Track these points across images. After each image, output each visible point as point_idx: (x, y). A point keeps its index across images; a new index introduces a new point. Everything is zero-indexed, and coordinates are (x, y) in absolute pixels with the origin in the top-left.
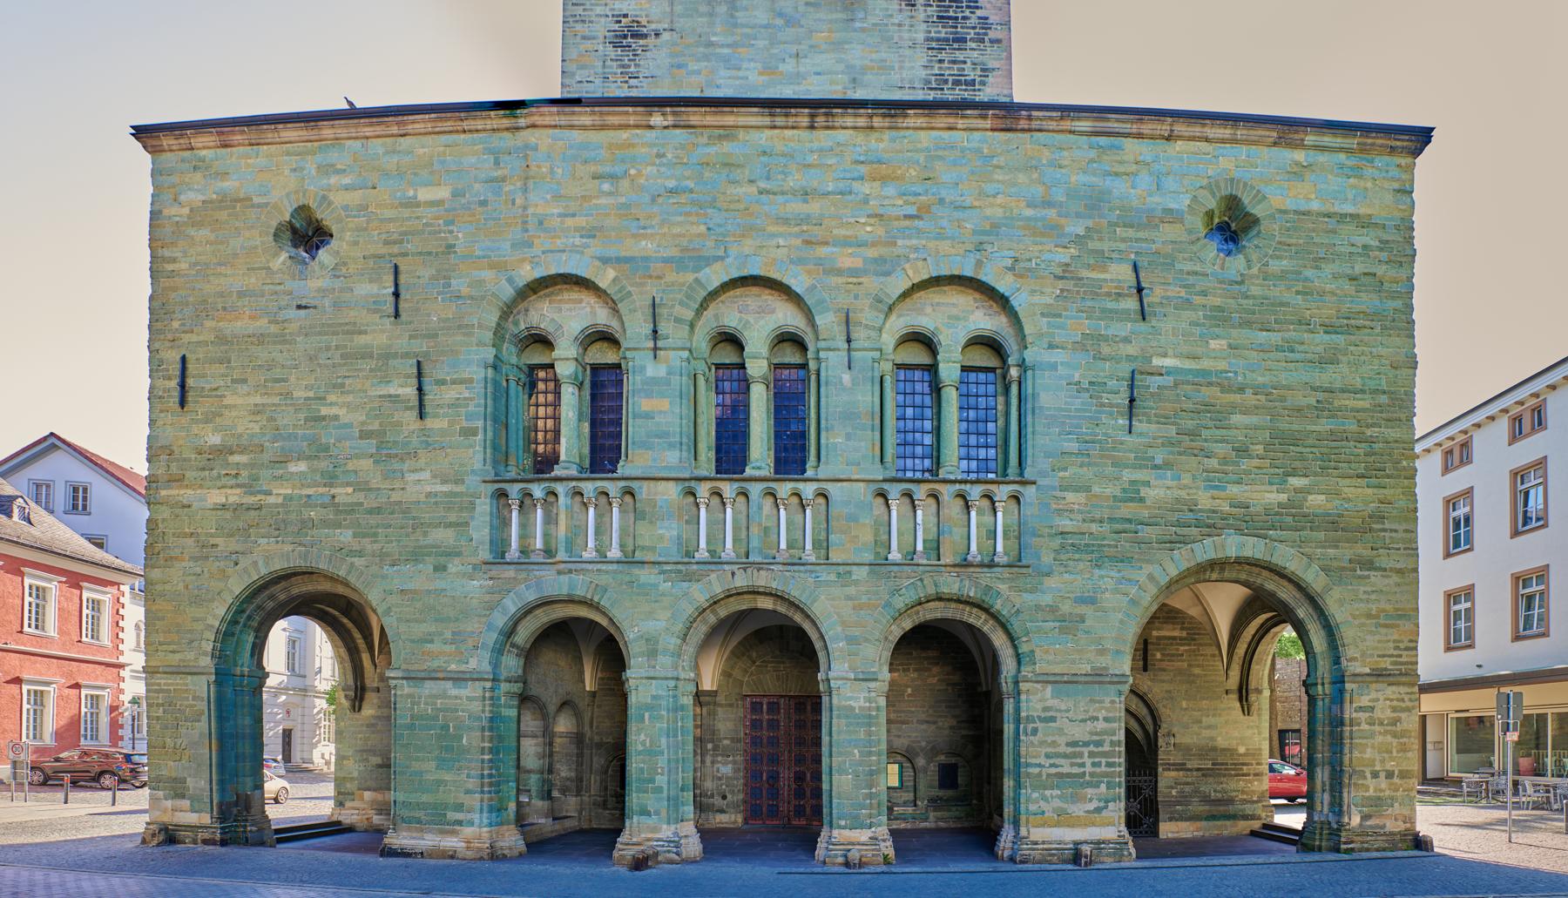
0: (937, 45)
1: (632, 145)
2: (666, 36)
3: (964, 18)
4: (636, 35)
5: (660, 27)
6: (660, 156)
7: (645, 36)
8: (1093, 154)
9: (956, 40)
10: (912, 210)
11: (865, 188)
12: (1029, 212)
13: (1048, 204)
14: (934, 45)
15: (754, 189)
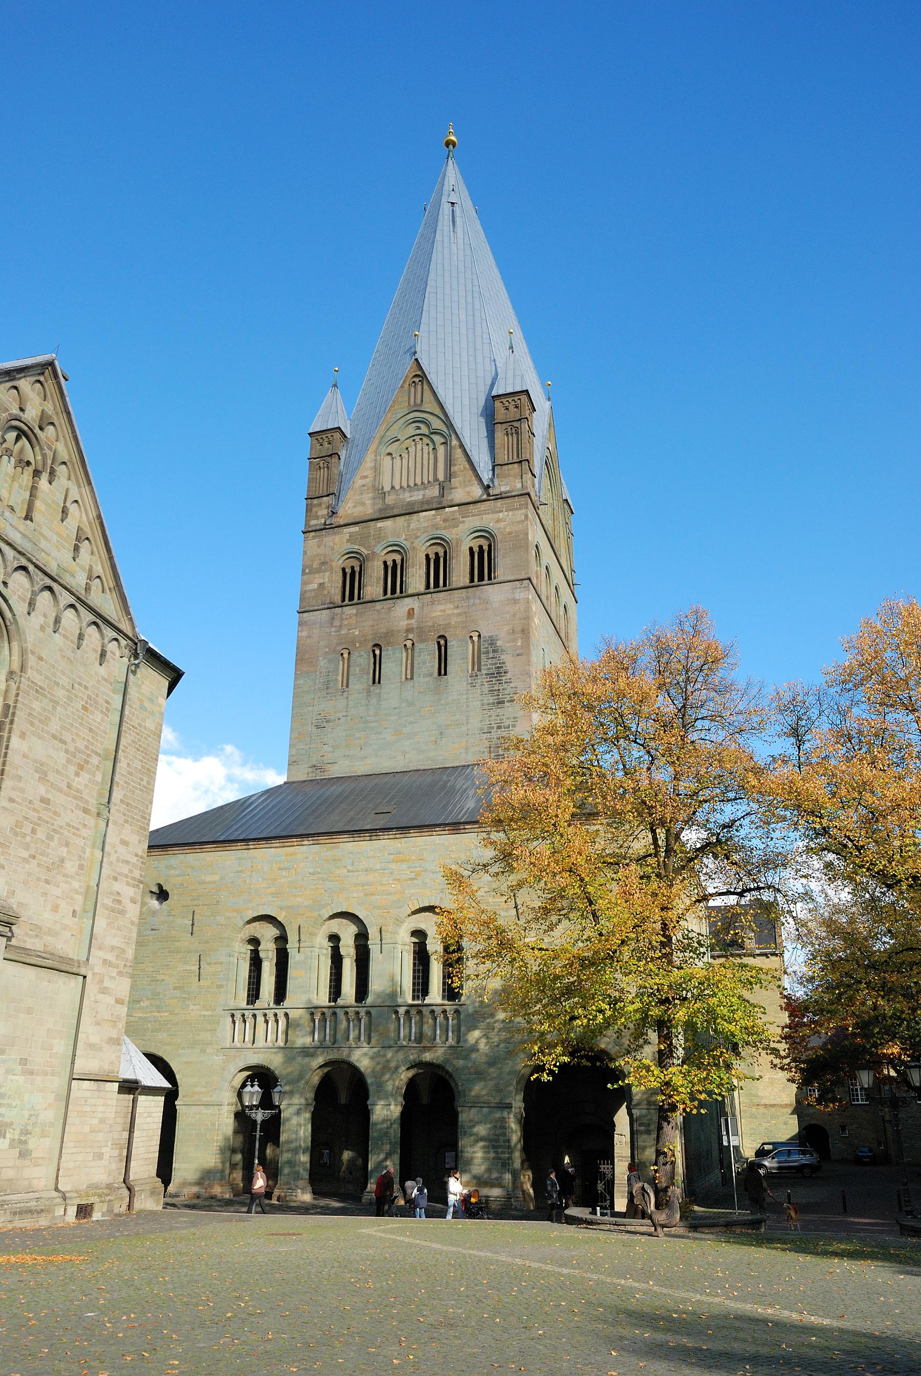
2: (343, 719)
5: (340, 715)
9: (499, 703)
14: (486, 707)
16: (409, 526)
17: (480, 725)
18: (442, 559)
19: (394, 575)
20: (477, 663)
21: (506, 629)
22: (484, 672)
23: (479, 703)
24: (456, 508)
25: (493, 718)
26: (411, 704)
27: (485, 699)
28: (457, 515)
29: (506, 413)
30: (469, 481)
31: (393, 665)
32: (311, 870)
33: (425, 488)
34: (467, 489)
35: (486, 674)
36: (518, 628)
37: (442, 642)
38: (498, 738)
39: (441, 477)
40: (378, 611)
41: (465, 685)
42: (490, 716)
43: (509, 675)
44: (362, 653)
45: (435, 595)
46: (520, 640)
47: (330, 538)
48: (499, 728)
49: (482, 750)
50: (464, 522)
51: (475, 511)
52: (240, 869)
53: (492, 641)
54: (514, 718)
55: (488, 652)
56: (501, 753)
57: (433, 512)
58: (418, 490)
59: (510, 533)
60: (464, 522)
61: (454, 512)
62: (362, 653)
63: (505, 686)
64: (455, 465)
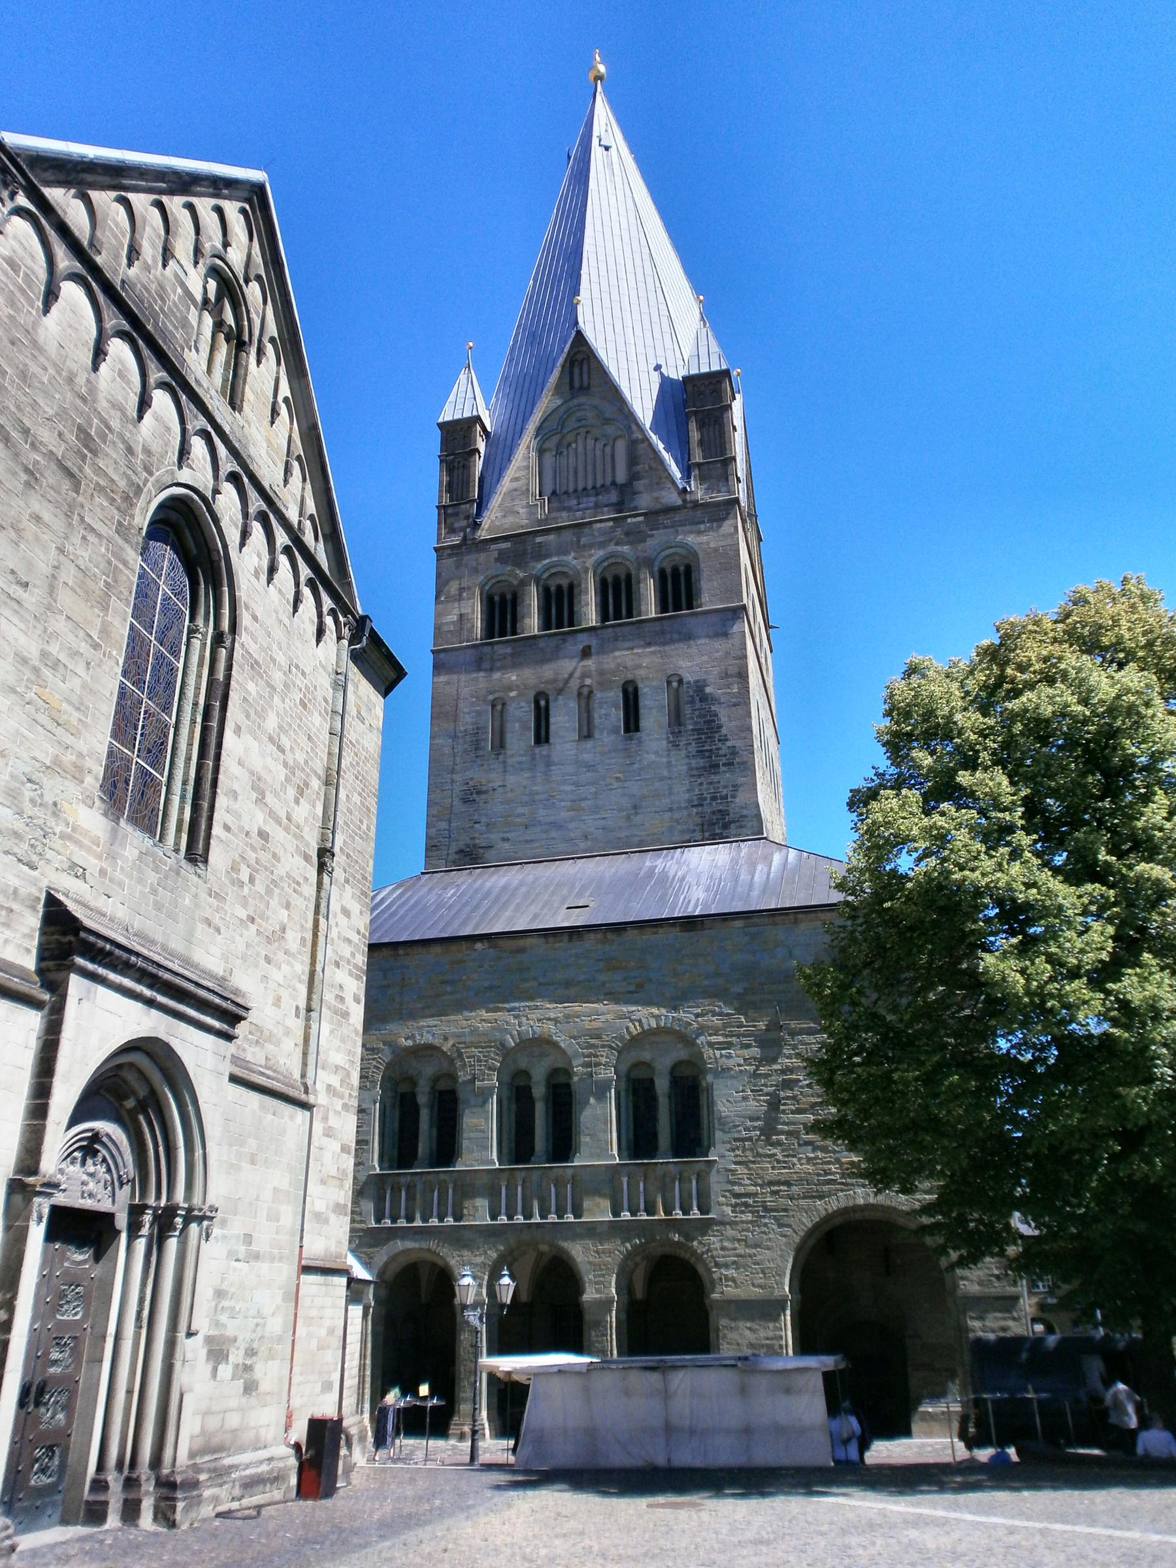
0: (696, 774)
1: (464, 961)
3: (718, 749)
4: (479, 793)
6: (480, 967)
7: (486, 792)
8: (747, 939)
10: (632, 988)
11: (602, 977)
12: (706, 982)
13: (717, 974)
15: (535, 984)
16: (579, 541)
17: (687, 796)
18: (623, 586)
19: (559, 605)
20: (676, 718)
21: (716, 671)
22: (690, 727)
23: (685, 767)
24: (641, 519)
25: (705, 786)
26: (590, 767)
27: (693, 762)
28: (643, 527)
29: (696, 402)
30: (658, 484)
31: (563, 719)
32: (486, 984)
33: (597, 495)
34: (656, 494)
35: (693, 730)
36: (733, 670)
37: (631, 689)
38: (713, 813)
39: (621, 477)
40: (542, 649)
41: (664, 743)
42: (701, 784)
43: (724, 731)
44: (523, 704)
45: (618, 629)
46: (736, 686)
47: (474, 556)
48: (714, 798)
49: (692, 827)
50: (652, 536)
51: (667, 522)
52: (385, 983)
53: (700, 687)
54: (734, 786)
55: (692, 702)
56: (718, 831)
57: (611, 524)
58: (588, 496)
59: (716, 550)
60: (652, 536)
61: (640, 522)
62: (523, 704)
63: (720, 745)
64: (637, 464)
